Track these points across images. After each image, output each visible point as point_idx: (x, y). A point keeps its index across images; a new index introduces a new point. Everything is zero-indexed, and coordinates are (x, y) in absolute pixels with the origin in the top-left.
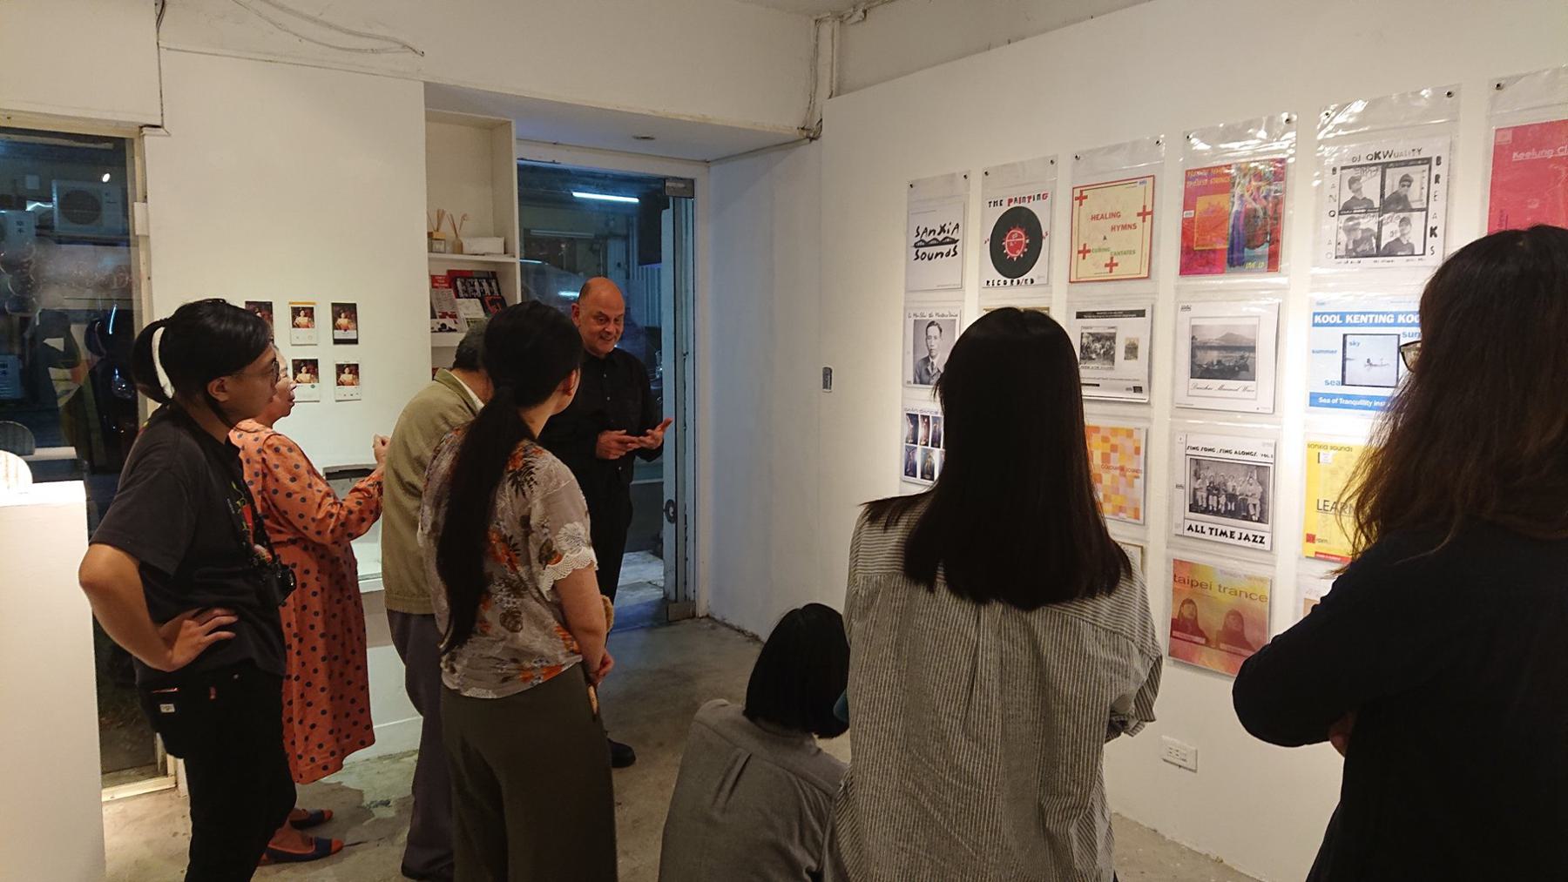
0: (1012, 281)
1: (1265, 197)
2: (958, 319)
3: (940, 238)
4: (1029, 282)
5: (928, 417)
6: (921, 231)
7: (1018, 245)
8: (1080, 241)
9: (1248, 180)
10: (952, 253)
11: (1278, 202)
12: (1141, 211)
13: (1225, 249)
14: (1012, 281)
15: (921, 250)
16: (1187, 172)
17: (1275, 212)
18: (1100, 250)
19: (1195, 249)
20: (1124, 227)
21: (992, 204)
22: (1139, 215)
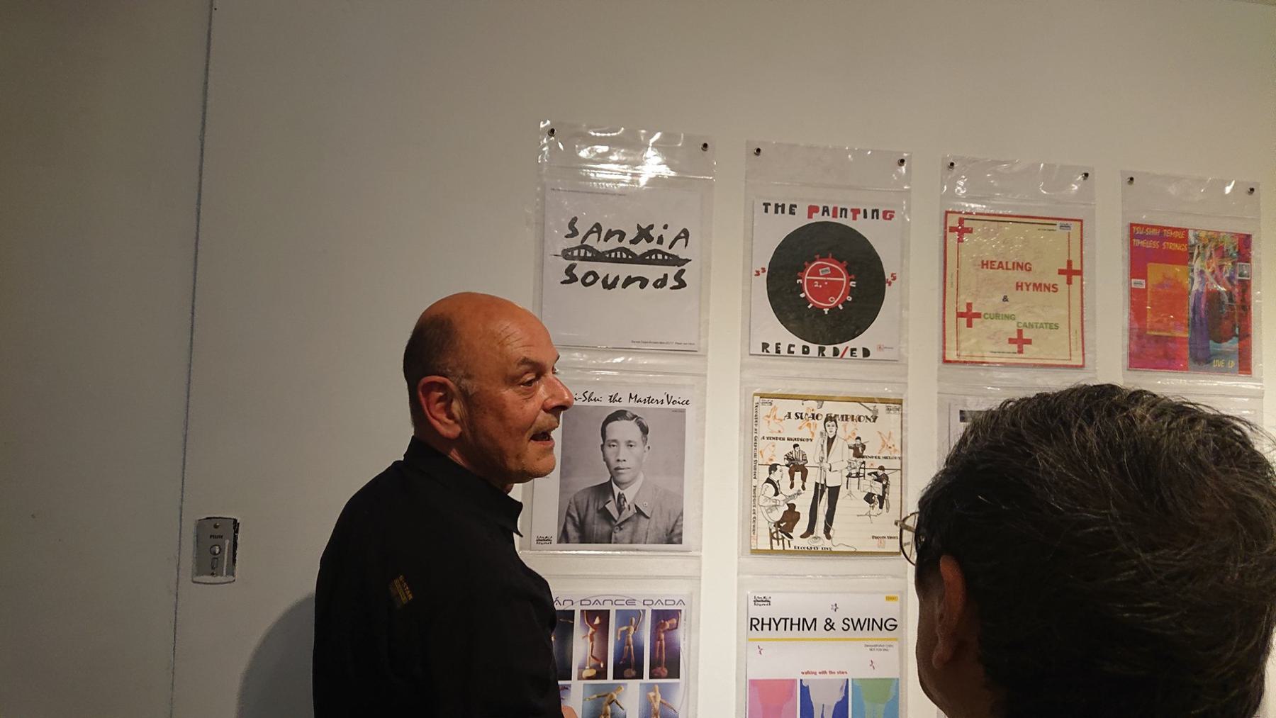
0: (821, 350)
1: (1230, 279)
2: (690, 412)
3: (641, 248)
4: (859, 353)
5: (605, 615)
6: (582, 229)
7: (834, 288)
8: (962, 297)
9: (1208, 254)
10: (671, 282)
11: (1245, 286)
12: (1065, 267)
13: (1186, 338)
14: (821, 350)
15: (582, 268)
16: (1132, 225)
17: (1243, 300)
18: (997, 316)
19: (1148, 333)
20: (1037, 287)
21: (771, 209)
22: (1061, 272)
